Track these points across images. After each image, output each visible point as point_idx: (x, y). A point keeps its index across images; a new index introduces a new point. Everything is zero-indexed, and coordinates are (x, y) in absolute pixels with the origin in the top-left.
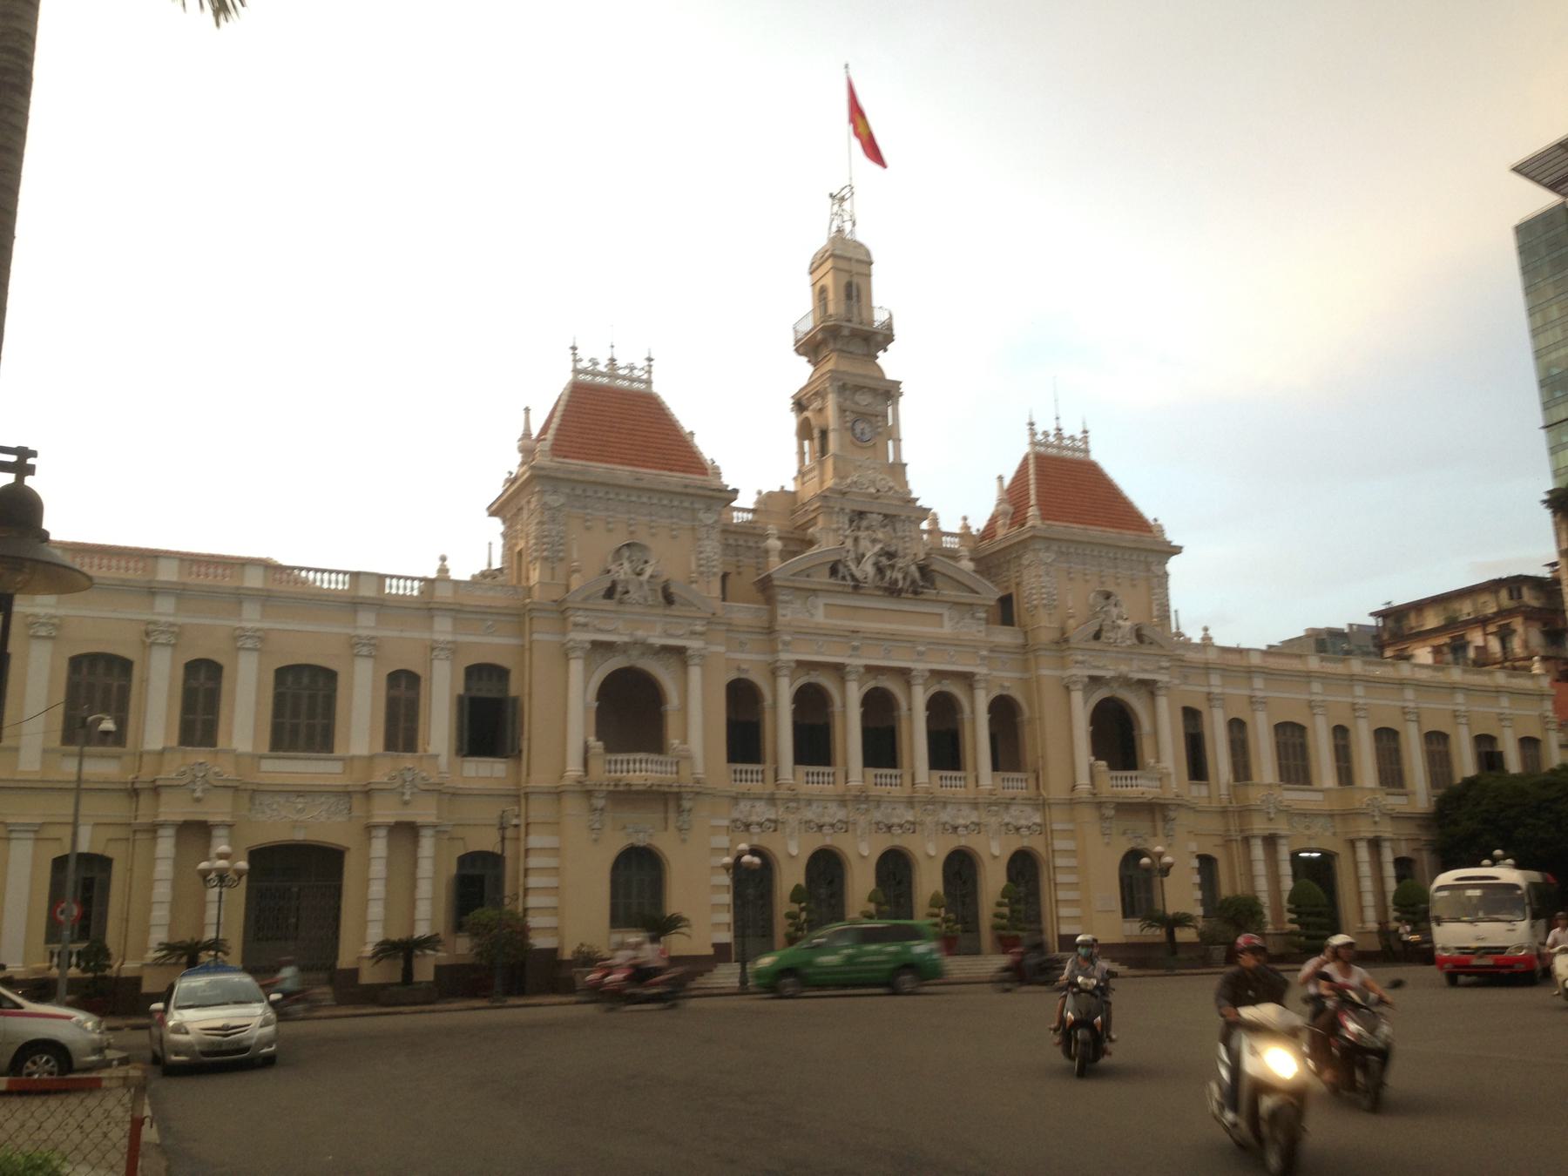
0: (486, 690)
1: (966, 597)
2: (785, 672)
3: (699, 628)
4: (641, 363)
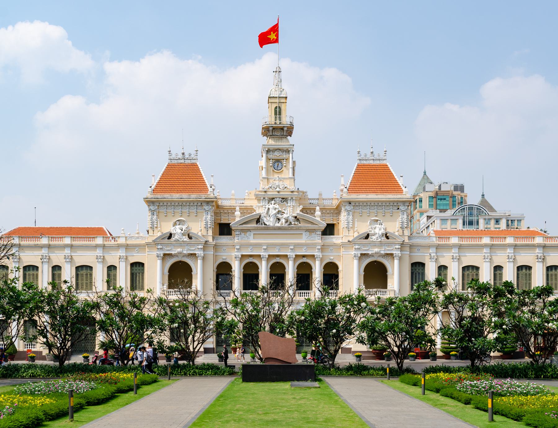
1: (310, 226)
3: (200, 247)
4: (193, 153)
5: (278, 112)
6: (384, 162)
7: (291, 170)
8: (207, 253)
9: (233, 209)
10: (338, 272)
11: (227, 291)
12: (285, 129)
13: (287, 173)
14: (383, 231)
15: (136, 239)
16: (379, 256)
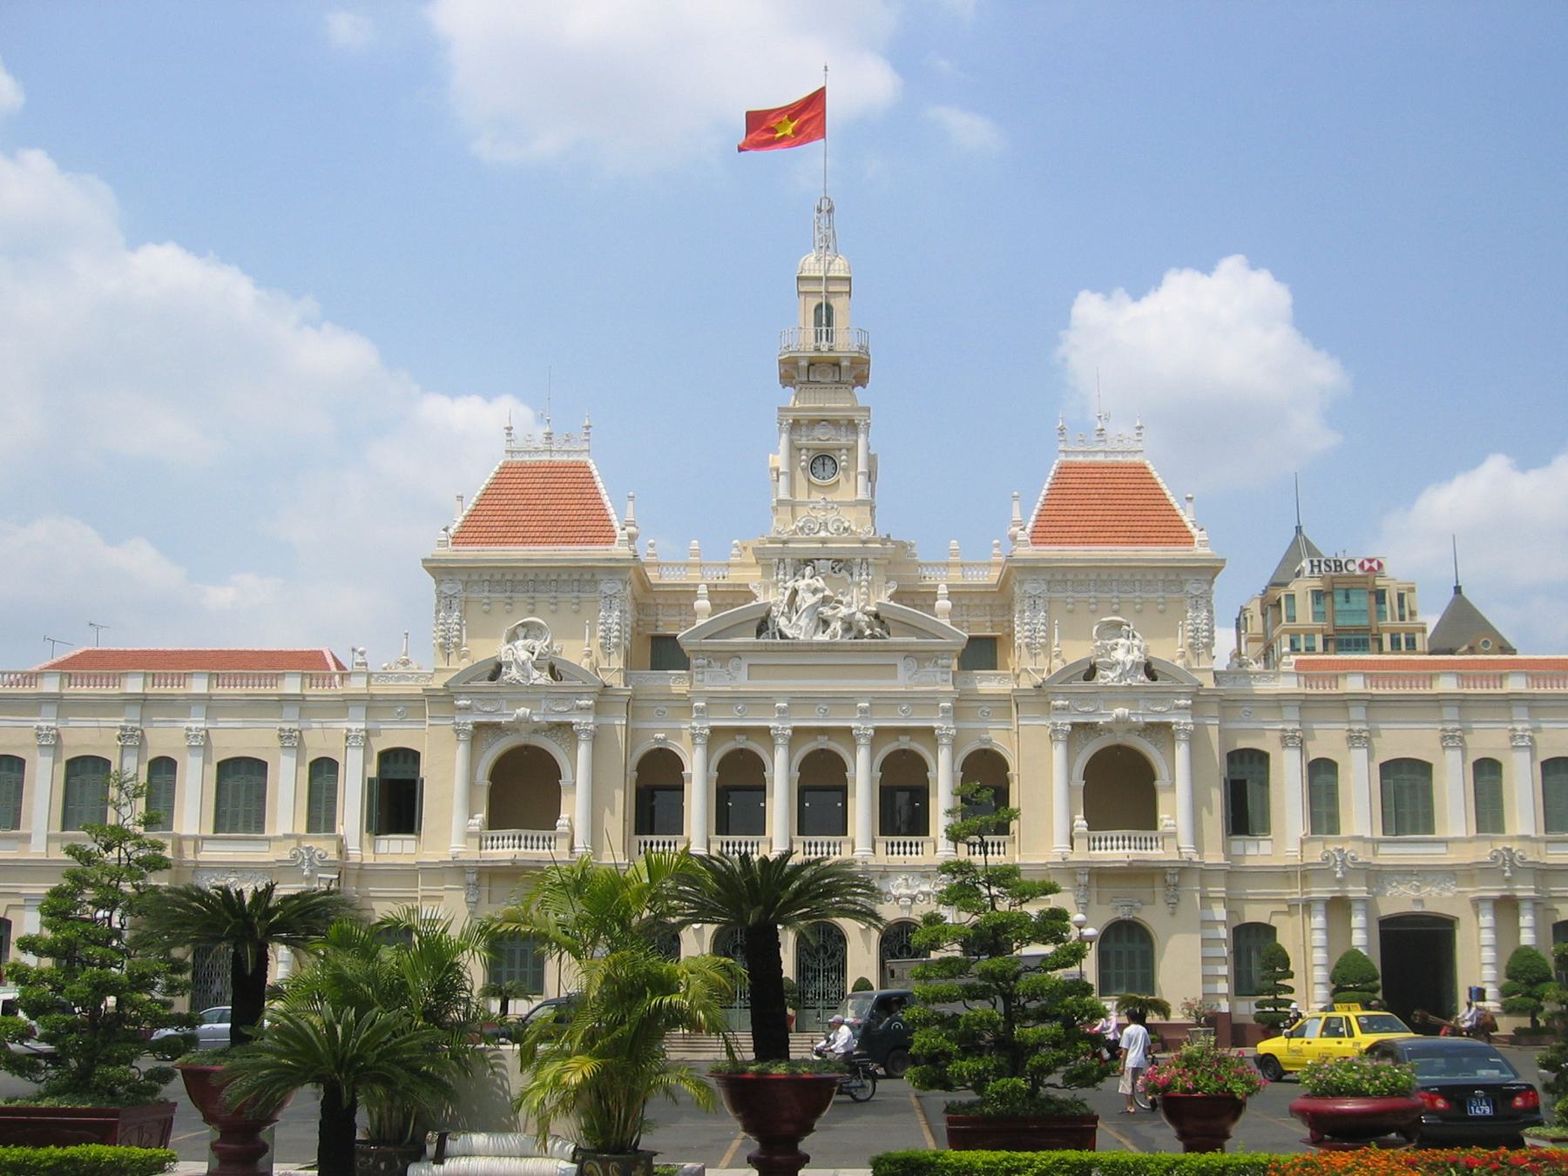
0: (399, 772)
2: (699, 740)
3: (583, 703)
5: (824, 316)
6: (1137, 459)
7: (861, 479)
8: (605, 721)
9: (690, 593)
12: (845, 363)
13: (852, 488)
14: (1136, 656)
15: (398, 679)
16: (1129, 731)
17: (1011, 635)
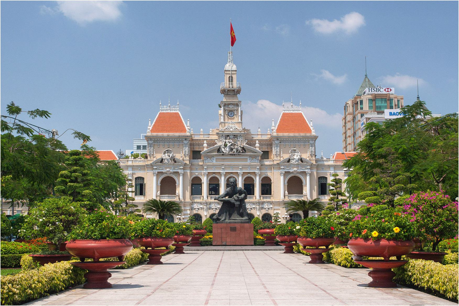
0: (140, 182)
5: (231, 79)
10: (271, 183)
11: (199, 196)
12: (236, 91)
13: (237, 119)
17: (272, 150)
